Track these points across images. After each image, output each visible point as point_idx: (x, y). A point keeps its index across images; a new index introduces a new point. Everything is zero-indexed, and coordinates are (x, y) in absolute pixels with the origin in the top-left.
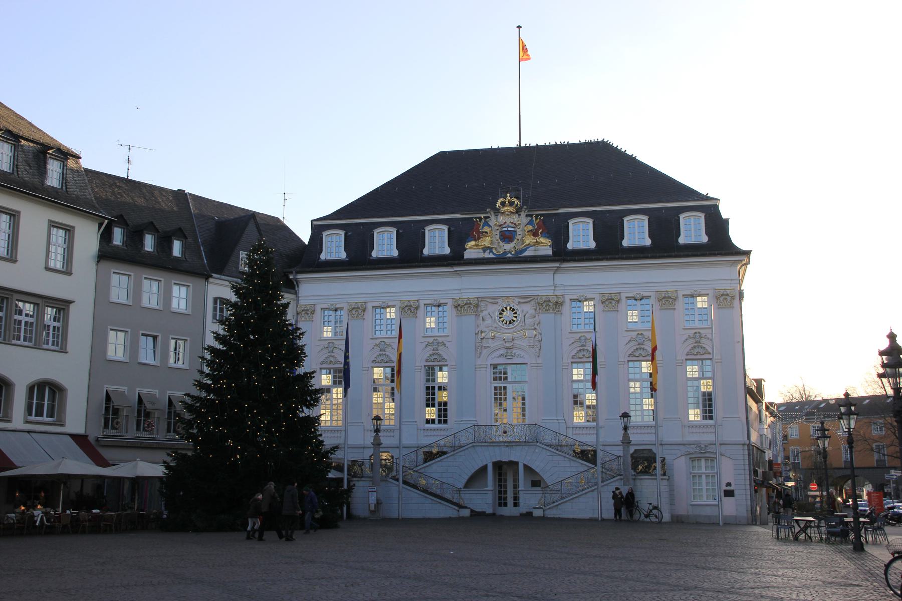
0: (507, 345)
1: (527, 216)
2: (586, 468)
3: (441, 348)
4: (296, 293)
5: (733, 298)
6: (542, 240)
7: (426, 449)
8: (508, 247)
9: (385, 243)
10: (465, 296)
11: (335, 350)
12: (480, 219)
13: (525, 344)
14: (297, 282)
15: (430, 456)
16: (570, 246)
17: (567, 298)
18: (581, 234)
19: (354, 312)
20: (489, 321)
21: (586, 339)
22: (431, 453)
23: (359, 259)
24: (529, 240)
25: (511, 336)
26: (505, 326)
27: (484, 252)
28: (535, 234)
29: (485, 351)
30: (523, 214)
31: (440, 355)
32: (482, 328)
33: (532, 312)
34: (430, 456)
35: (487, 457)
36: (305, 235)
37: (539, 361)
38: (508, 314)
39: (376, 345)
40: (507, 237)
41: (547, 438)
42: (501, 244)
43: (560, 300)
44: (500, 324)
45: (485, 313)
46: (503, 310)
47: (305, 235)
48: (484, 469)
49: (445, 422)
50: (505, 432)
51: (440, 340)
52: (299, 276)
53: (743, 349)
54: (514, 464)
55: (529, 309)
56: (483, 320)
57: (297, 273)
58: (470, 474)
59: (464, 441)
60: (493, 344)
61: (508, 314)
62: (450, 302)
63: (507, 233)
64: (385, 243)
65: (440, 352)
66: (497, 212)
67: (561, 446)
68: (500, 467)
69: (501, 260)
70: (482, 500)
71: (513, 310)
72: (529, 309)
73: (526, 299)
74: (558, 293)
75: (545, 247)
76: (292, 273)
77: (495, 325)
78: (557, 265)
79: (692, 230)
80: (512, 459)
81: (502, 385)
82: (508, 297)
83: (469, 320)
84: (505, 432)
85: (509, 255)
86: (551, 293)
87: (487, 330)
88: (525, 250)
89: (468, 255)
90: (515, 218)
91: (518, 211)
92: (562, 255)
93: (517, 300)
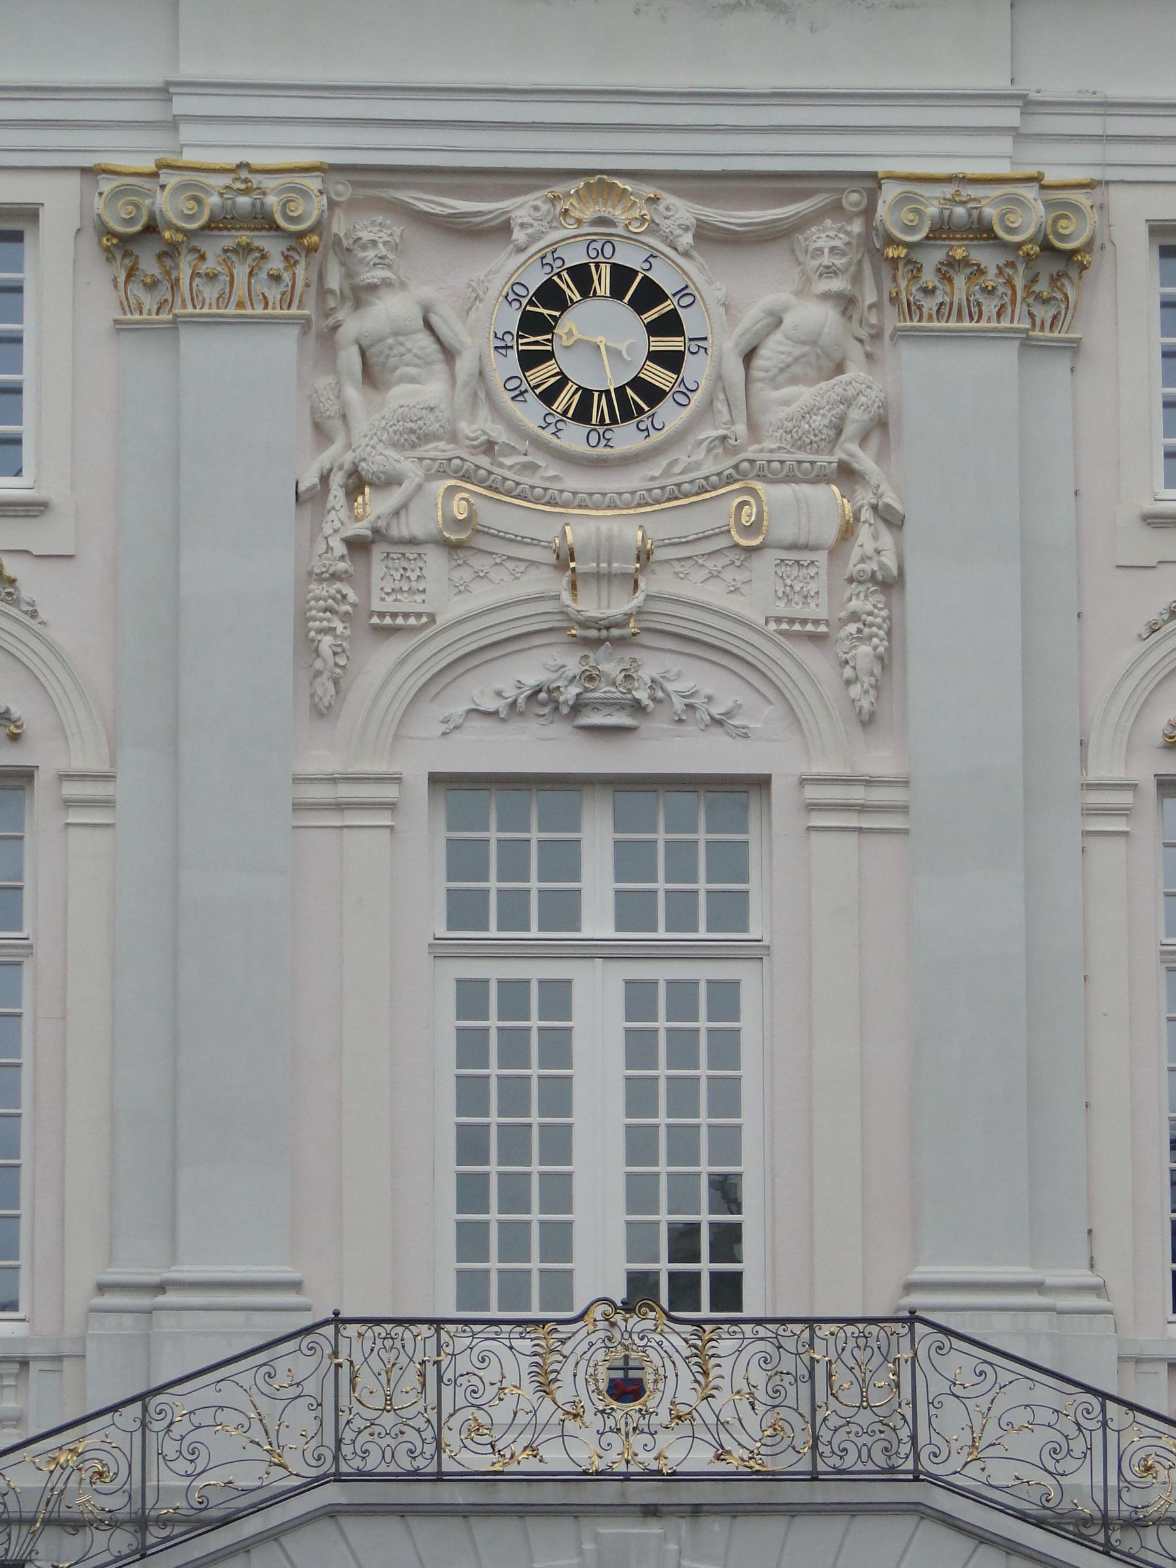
0: (591, 605)
10: (207, 148)
13: (749, 598)
17: (1130, 218)
20: (422, 391)
26: (574, 437)
32: (368, 436)
37: (878, 760)
38: (602, 341)
43: (1074, 233)
44: (531, 413)
45: (391, 310)
46: (550, 294)
50: (626, 1389)
56: (372, 375)
59: (233, 1464)
60: (451, 596)
61: (602, 341)
62: (61, 206)
67: (1134, 1524)
71: (649, 295)
77: (483, 425)
81: (535, 971)
82: (600, 183)
83: (244, 373)
84: (626, 1389)
86: (991, 158)
87: (408, 466)
93: (681, 211)
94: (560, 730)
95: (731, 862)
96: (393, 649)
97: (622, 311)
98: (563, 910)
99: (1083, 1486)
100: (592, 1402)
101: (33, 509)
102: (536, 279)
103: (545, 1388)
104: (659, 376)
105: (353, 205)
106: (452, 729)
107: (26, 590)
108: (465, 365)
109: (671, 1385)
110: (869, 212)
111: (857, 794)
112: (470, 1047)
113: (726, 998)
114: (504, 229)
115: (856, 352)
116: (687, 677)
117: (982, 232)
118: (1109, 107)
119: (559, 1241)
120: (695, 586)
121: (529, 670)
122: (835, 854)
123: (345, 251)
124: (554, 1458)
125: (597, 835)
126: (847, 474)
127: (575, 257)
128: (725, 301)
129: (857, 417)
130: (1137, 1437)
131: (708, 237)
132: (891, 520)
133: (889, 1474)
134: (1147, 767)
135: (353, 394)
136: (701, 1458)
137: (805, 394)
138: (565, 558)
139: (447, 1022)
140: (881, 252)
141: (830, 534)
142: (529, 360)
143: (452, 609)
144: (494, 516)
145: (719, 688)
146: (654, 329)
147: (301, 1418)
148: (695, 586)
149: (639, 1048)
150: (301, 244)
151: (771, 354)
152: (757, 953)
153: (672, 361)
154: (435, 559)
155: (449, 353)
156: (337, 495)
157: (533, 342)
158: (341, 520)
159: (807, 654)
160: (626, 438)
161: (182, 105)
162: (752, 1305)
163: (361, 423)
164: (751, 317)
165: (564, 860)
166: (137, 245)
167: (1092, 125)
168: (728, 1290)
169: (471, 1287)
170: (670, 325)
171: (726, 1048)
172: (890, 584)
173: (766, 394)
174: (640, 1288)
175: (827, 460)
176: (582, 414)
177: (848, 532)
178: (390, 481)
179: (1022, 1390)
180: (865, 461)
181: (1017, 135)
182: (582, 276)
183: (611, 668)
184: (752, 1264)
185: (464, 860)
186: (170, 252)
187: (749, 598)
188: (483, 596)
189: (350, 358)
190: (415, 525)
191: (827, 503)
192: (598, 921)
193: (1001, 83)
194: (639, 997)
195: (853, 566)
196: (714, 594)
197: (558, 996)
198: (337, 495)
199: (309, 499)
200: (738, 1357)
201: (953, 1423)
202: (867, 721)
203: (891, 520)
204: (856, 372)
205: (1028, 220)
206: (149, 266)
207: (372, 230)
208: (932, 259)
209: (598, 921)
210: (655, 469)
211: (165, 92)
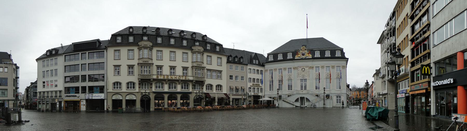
9: (280, 57)
16: (315, 56)
18: (317, 54)
23: (276, 60)
34: (288, 96)
35: (299, 96)
36: (266, 56)
38: (303, 70)
40: (303, 55)
47: (266, 56)
48: (298, 98)
54: (304, 98)
55: (307, 69)
60: (300, 75)
61: (303, 70)
64: (280, 57)
68: (301, 98)
70: (298, 104)
72: (307, 69)
73: (307, 67)
75: (310, 56)
83: (296, 71)
89: (296, 58)
90: (305, 51)
92: (314, 58)
128: (306, 69)
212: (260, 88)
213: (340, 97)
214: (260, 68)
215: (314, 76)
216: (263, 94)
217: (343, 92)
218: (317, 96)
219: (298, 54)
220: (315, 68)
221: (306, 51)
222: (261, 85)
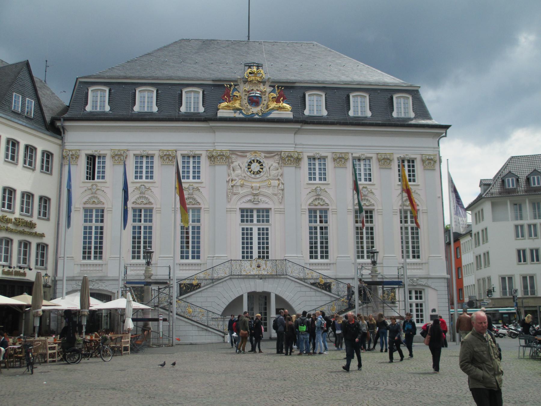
0: (254, 192)
1: (270, 86)
2: (328, 299)
3: (197, 192)
4: (62, 139)
5: (435, 162)
6: (284, 104)
7: (187, 282)
8: (255, 110)
10: (218, 148)
11: (98, 192)
12: (231, 86)
14: (64, 129)
15: (187, 288)
19: (117, 158)
20: (238, 172)
21: (321, 190)
22: (192, 285)
24: (273, 105)
25: (258, 185)
26: (253, 176)
27: (235, 113)
28: (278, 101)
29: (235, 197)
30: (268, 84)
31: (194, 199)
32: (233, 175)
33: (275, 165)
37: (282, 207)
38: (255, 167)
39: (136, 188)
40: (254, 101)
41: (295, 272)
42: (249, 107)
43: (300, 157)
44: (249, 173)
45: (236, 164)
46: (251, 162)
49: (198, 257)
50: (259, 267)
51: (195, 186)
52: (67, 124)
53: (443, 203)
56: (233, 170)
57: (66, 120)
58: (227, 304)
59: (221, 274)
60: (241, 191)
61: (255, 167)
63: (255, 99)
65: (195, 196)
66: (246, 81)
67: (307, 279)
68: (252, 296)
69: (250, 119)
71: (260, 162)
73: (270, 154)
74: (299, 150)
76: (59, 120)
77: (244, 175)
78: (298, 126)
79: (402, 108)
80: (265, 290)
82: (255, 152)
83: (221, 170)
85: (256, 116)
86: (292, 149)
88: (270, 113)
89: (221, 113)
90: (262, 87)
91: (264, 82)
93: (263, 155)
94: (251, 204)
95: (268, 216)
96: (236, 196)
97: (257, 164)
98: (252, 221)
99: (302, 276)
100: (256, 268)
101: (202, 183)
102: (249, 161)
103: (251, 266)
104: (261, 170)
105: (232, 154)
106: (241, 203)
107: (201, 190)
108: (243, 169)
109: (263, 266)
110: (281, 155)
111: (280, 210)
112: (243, 234)
113: (267, 229)
114: (246, 156)
115: (279, 168)
116: (263, 199)
117: (291, 157)
118: (303, 145)
119: (251, 252)
120: (264, 190)
121: (249, 198)
122: (278, 216)
123: (231, 158)
124: (252, 273)
125: (255, 214)
126: (279, 179)
127: (253, 159)
128: (267, 163)
129: (280, 174)
130: (307, 271)
131: (265, 157)
132: (283, 184)
133: (283, 275)
134: (307, 207)
135: (232, 172)
136: (266, 273)
137: (275, 172)
138: (252, 187)
139: (241, 232)
140: (281, 158)
141: (277, 185)
142: (249, 169)
143: (241, 192)
144: (245, 183)
145: (267, 200)
146: (260, 166)
147: (228, 269)
148: (264, 190)
149: (259, 234)
150: (228, 157)
151: (272, 168)
152: (270, 225)
153: (262, 169)
154: (240, 188)
155: (241, 168)
156: (230, 181)
157: (249, 167)
158: (231, 184)
159: (275, 196)
160: (258, 176)
161: (216, 144)
162: (270, 259)
163: (233, 174)
164: (270, 165)
165: (252, 216)
166: (212, 158)
167: (302, 147)
168: (268, 257)
169: (243, 257)
170: (262, 165)
171: (267, 234)
172: (283, 190)
173: (271, 172)
174: (259, 257)
175: (277, 178)
176: (254, 174)
177: (279, 185)
178: (236, 180)
179: (296, 266)
180: (280, 178)
181: (295, 148)
182: (254, 161)
183: (256, 198)
184: (270, 255)
185: (242, 216)
186: (214, 158)
187: (270, 191)
188: (244, 191)
189: (232, 168)
190: (238, 184)
191: (277, 182)
192: (255, 221)
193: (293, 143)
194: (259, 229)
195: (279, 188)
196: (266, 191)
197: (251, 229)
198: (230, 181)
199: (228, 182)
200: (269, 263)
201: (289, 270)
202: (281, 203)
203: (283, 184)
204: (279, 170)
205: (296, 155)
206: (212, 159)
207: (234, 156)
208: (287, 159)
209: (255, 221)
210: (260, 179)
211: (214, 143)
212: (34, 242)
213: (419, 294)
214: (43, 143)
215: (306, 201)
216: (50, 272)
217: (433, 274)
218: (327, 287)
219: (230, 98)
220: (305, 163)
221: (269, 89)
222: (41, 226)
